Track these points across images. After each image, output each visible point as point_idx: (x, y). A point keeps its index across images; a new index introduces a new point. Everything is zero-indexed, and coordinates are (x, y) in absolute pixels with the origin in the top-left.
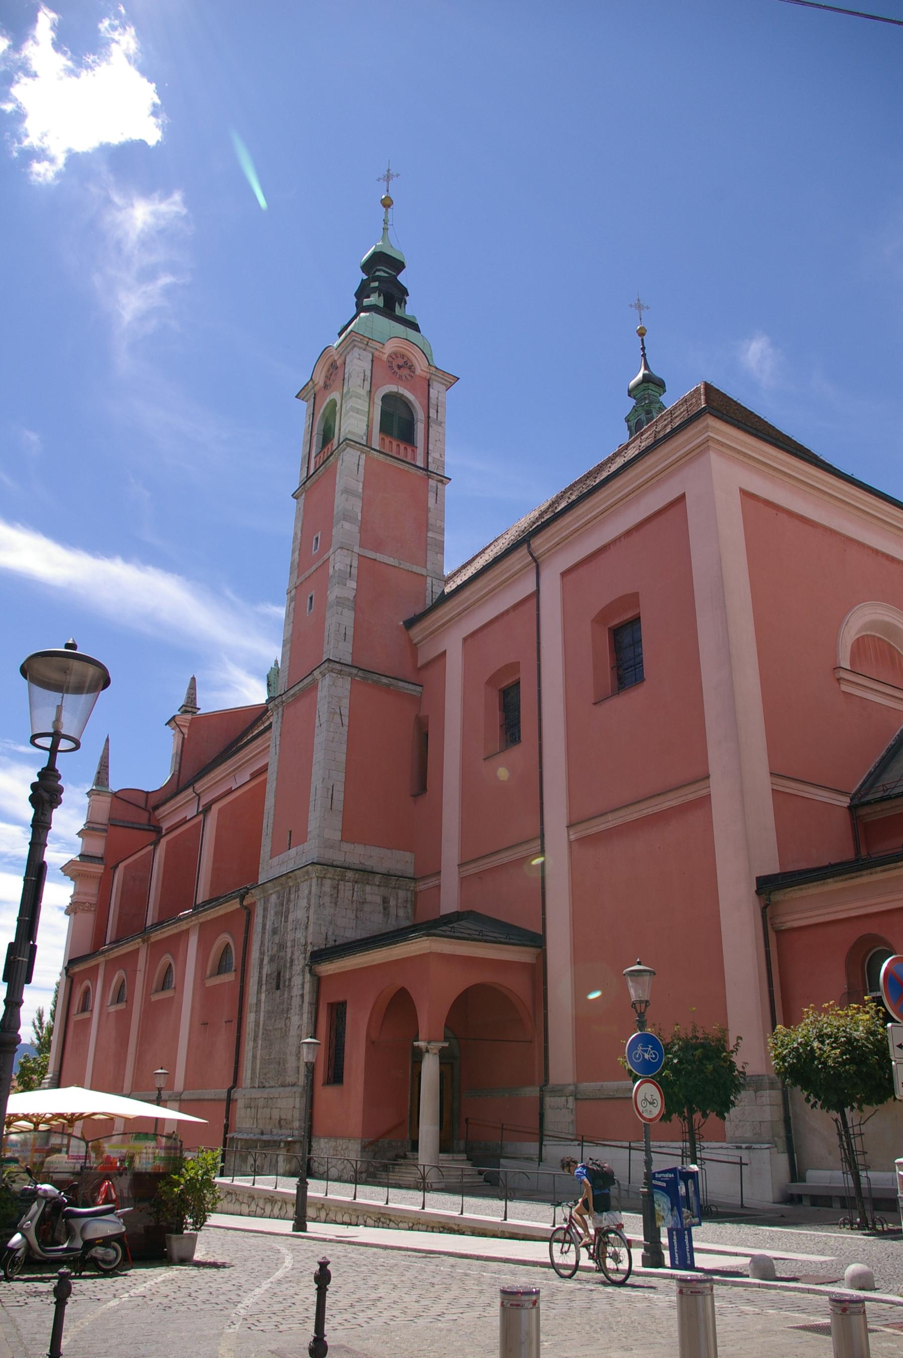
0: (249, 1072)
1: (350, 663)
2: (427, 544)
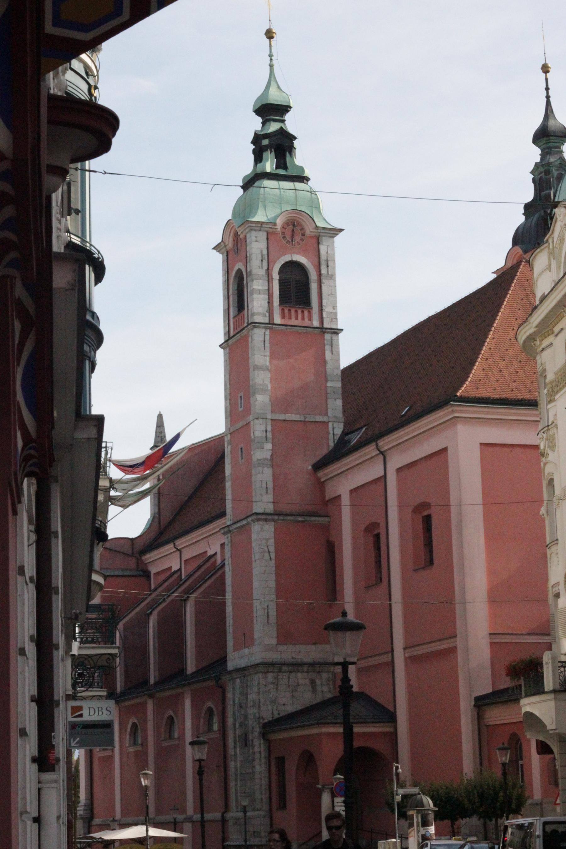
0: (234, 801)
1: (272, 512)
2: (327, 394)
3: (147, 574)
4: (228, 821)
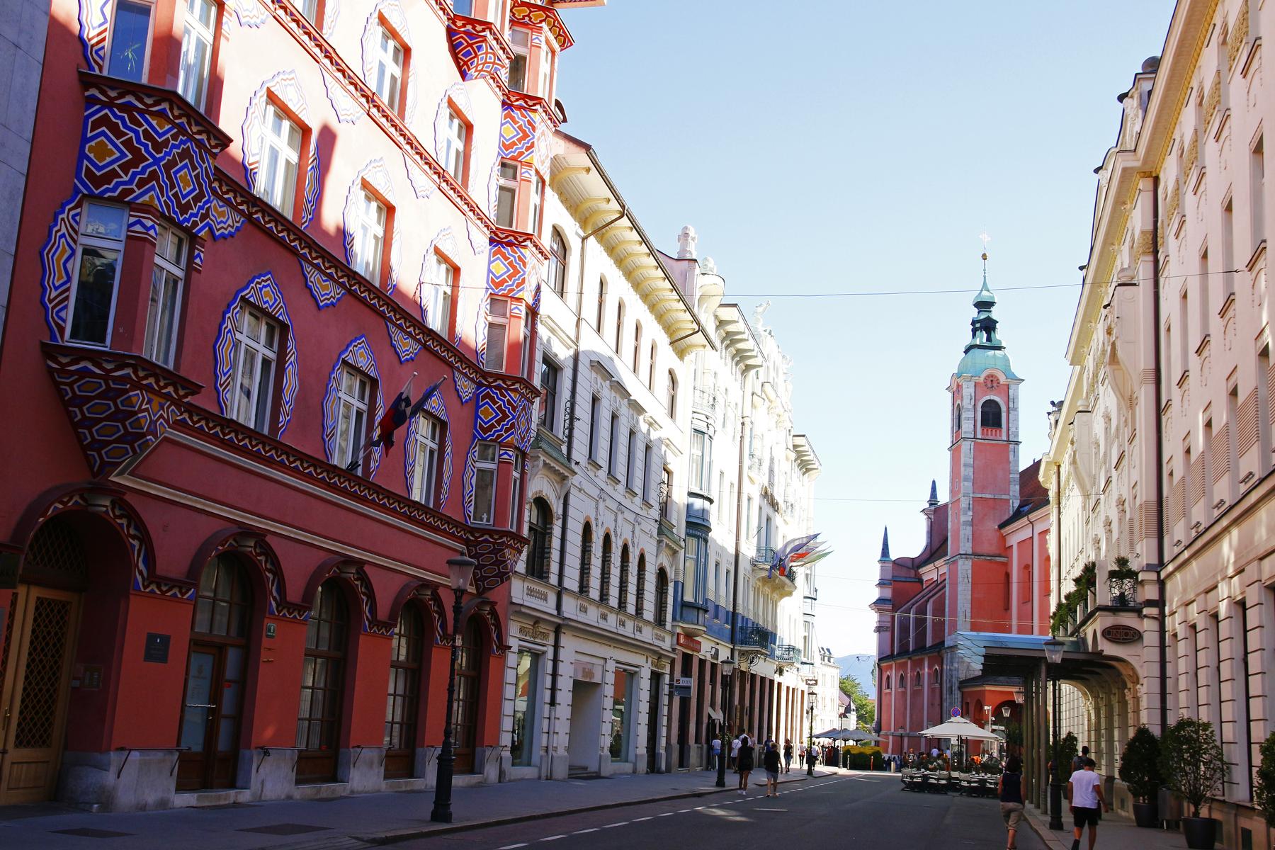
2: (1009, 482)
3: (921, 581)
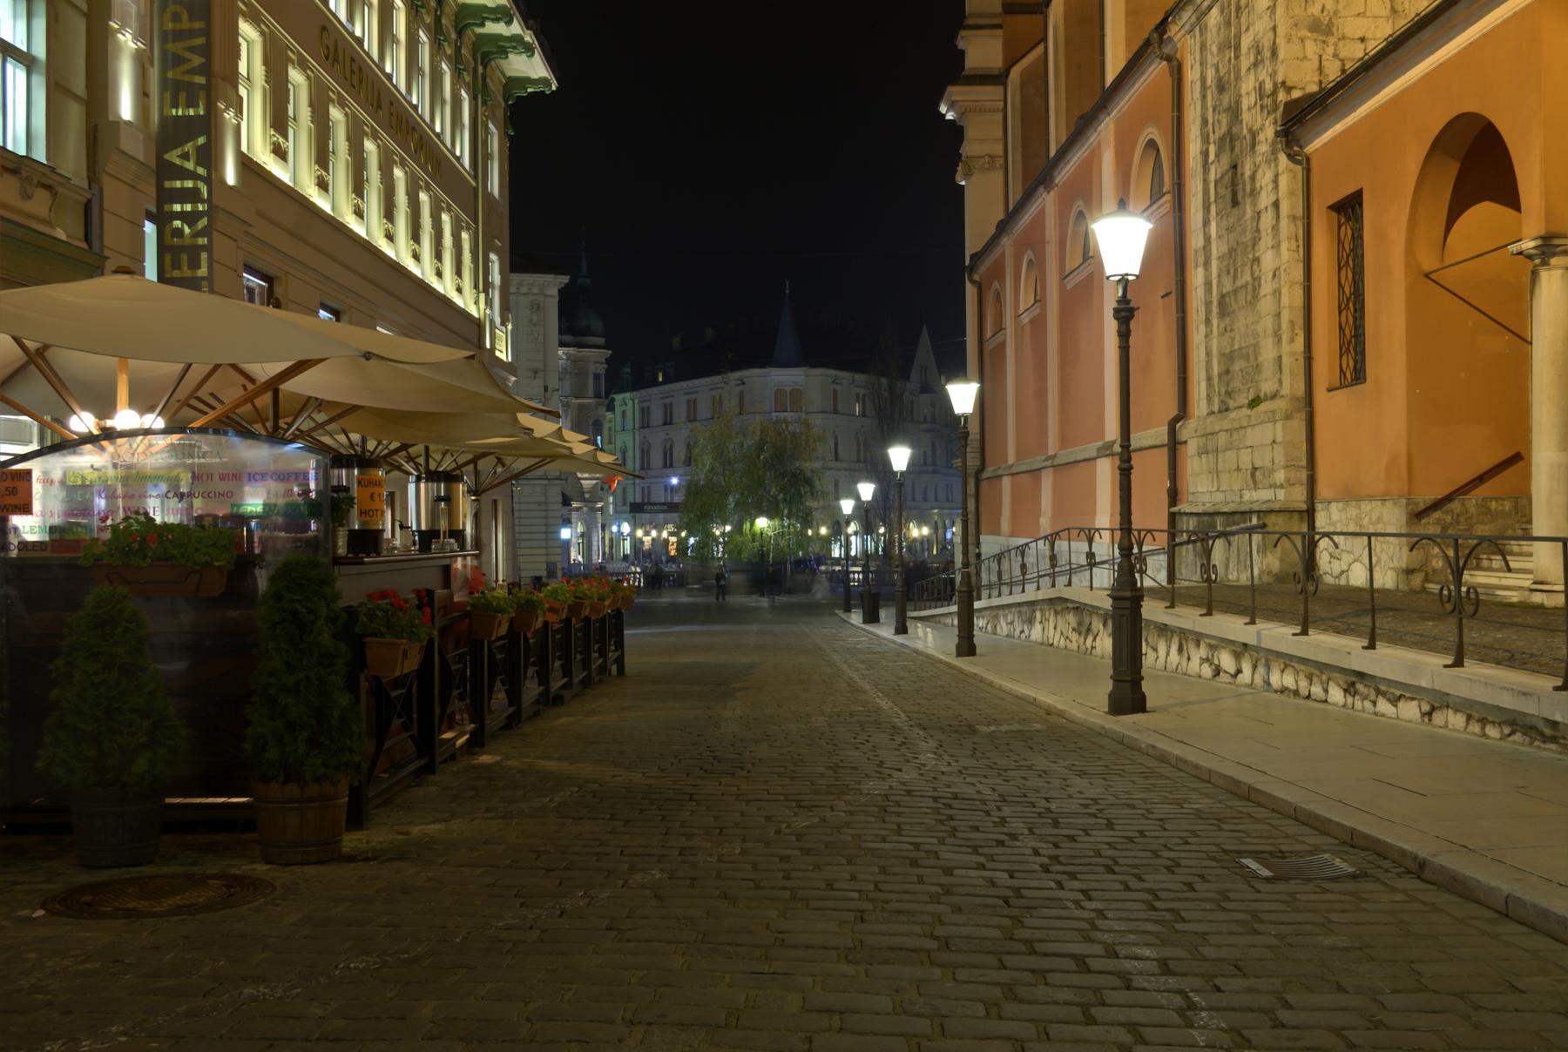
0: (1203, 385)
4: (1186, 442)
